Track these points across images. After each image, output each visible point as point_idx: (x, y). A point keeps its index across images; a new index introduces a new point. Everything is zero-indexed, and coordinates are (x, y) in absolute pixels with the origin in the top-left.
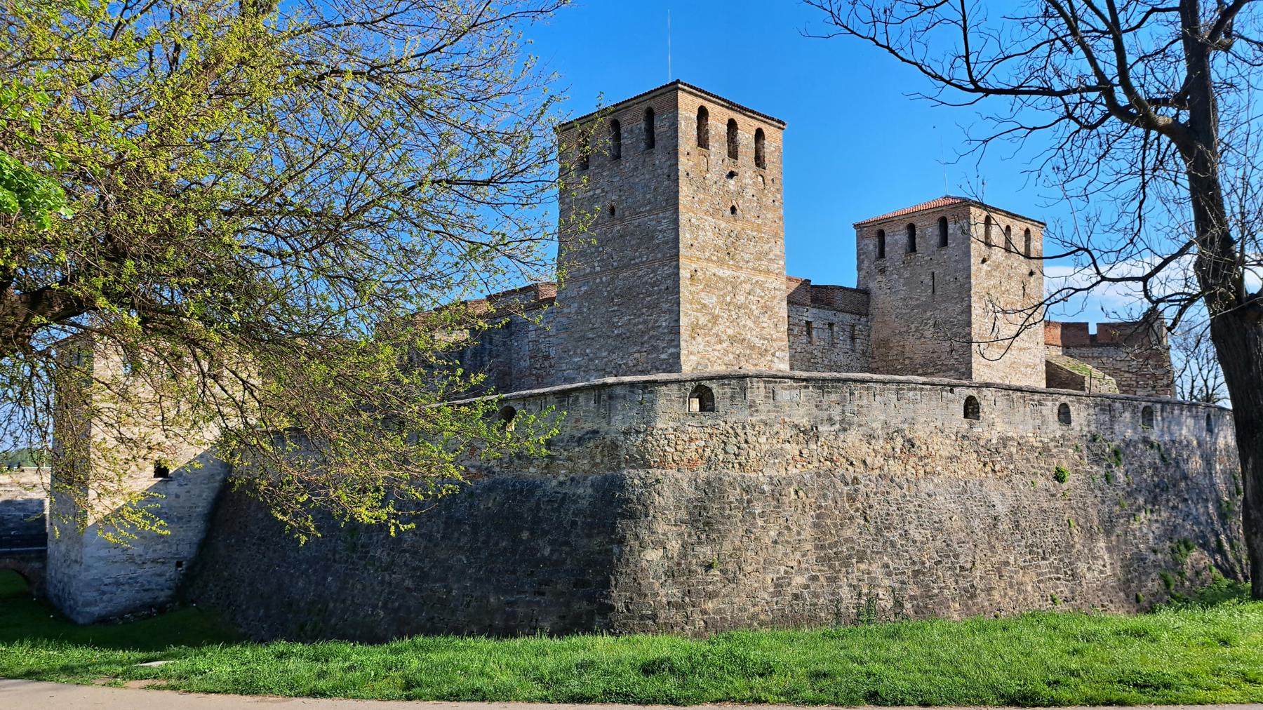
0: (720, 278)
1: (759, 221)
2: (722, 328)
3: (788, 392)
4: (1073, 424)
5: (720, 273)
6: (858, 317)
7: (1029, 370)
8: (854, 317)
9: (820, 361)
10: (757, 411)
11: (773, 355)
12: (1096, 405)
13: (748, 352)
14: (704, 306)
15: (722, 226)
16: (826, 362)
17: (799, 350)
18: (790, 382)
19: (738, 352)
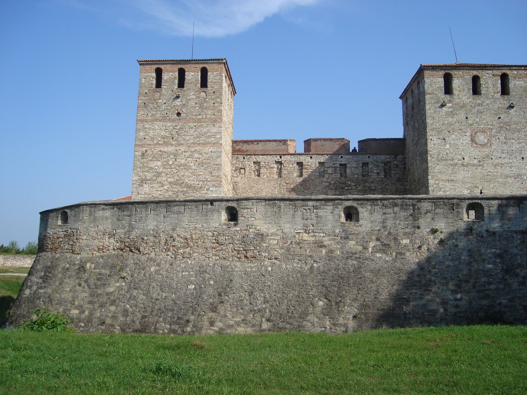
0: (165, 152)
1: (200, 117)
2: (164, 179)
3: (102, 212)
4: (361, 222)
5: (166, 149)
6: (393, 156)
7: (510, 180)
8: (389, 156)
9: (354, 188)
10: (84, 223)
11: (208, 190)
12: (396, 205)
13: (185, 189)
14: (151, 168)
15: (169, 124)
16: (359, 188)
17: (333, 182)
18: (103, 207)
19: (176, 190)
